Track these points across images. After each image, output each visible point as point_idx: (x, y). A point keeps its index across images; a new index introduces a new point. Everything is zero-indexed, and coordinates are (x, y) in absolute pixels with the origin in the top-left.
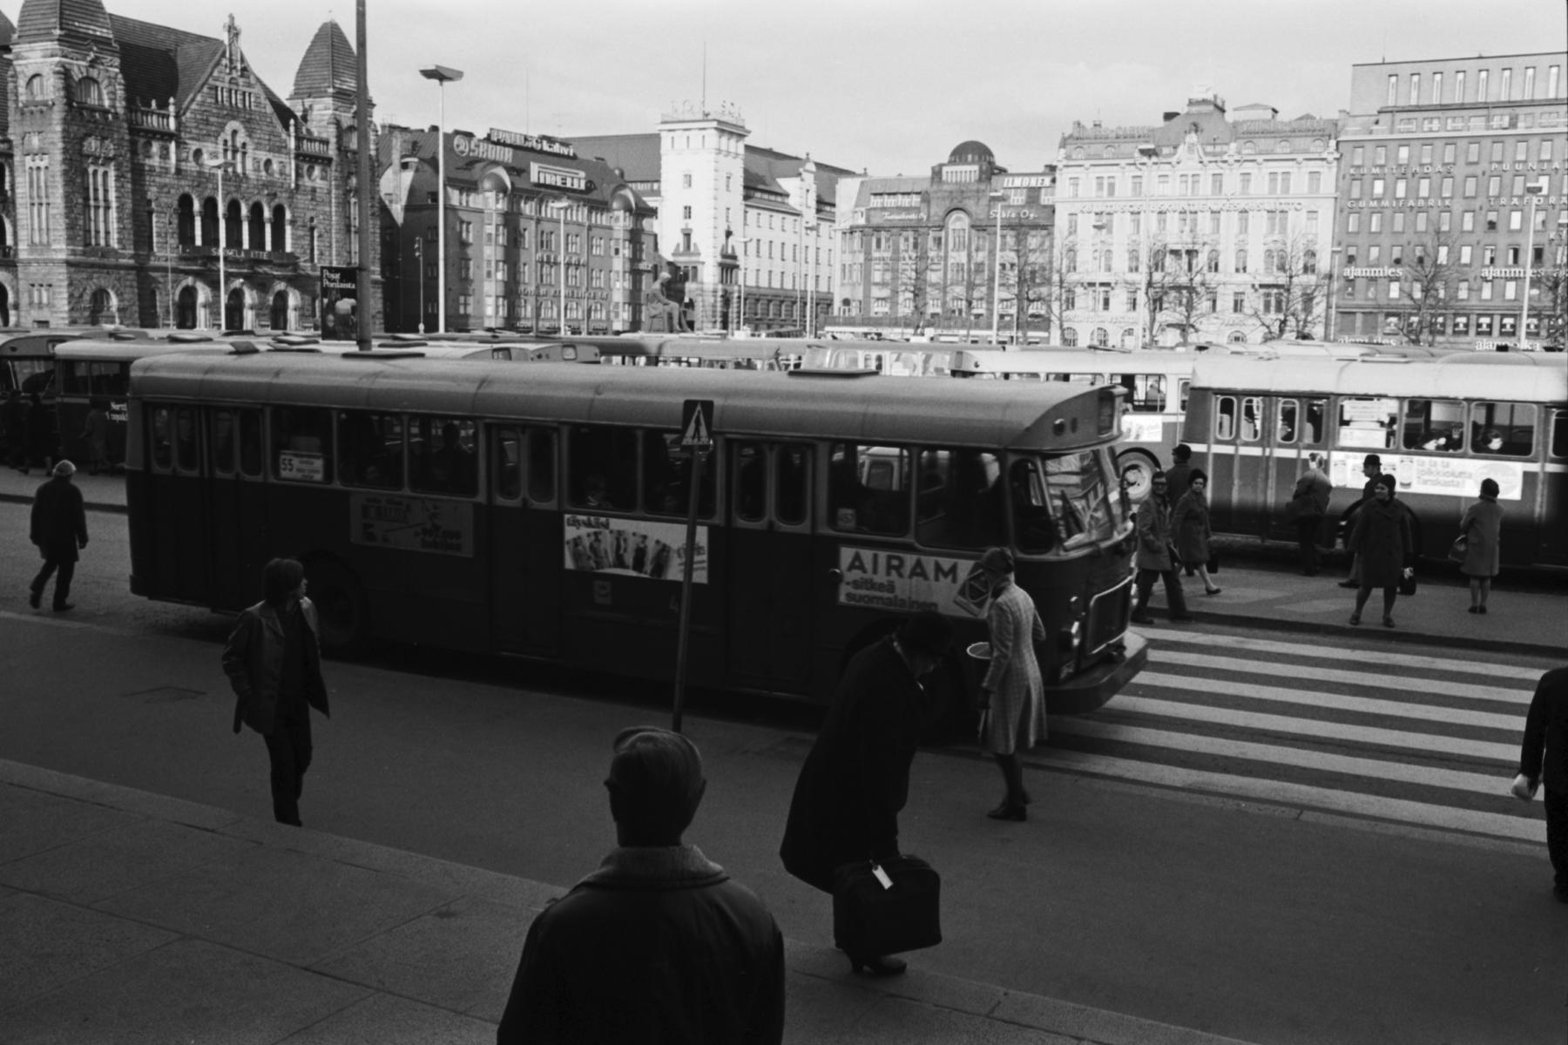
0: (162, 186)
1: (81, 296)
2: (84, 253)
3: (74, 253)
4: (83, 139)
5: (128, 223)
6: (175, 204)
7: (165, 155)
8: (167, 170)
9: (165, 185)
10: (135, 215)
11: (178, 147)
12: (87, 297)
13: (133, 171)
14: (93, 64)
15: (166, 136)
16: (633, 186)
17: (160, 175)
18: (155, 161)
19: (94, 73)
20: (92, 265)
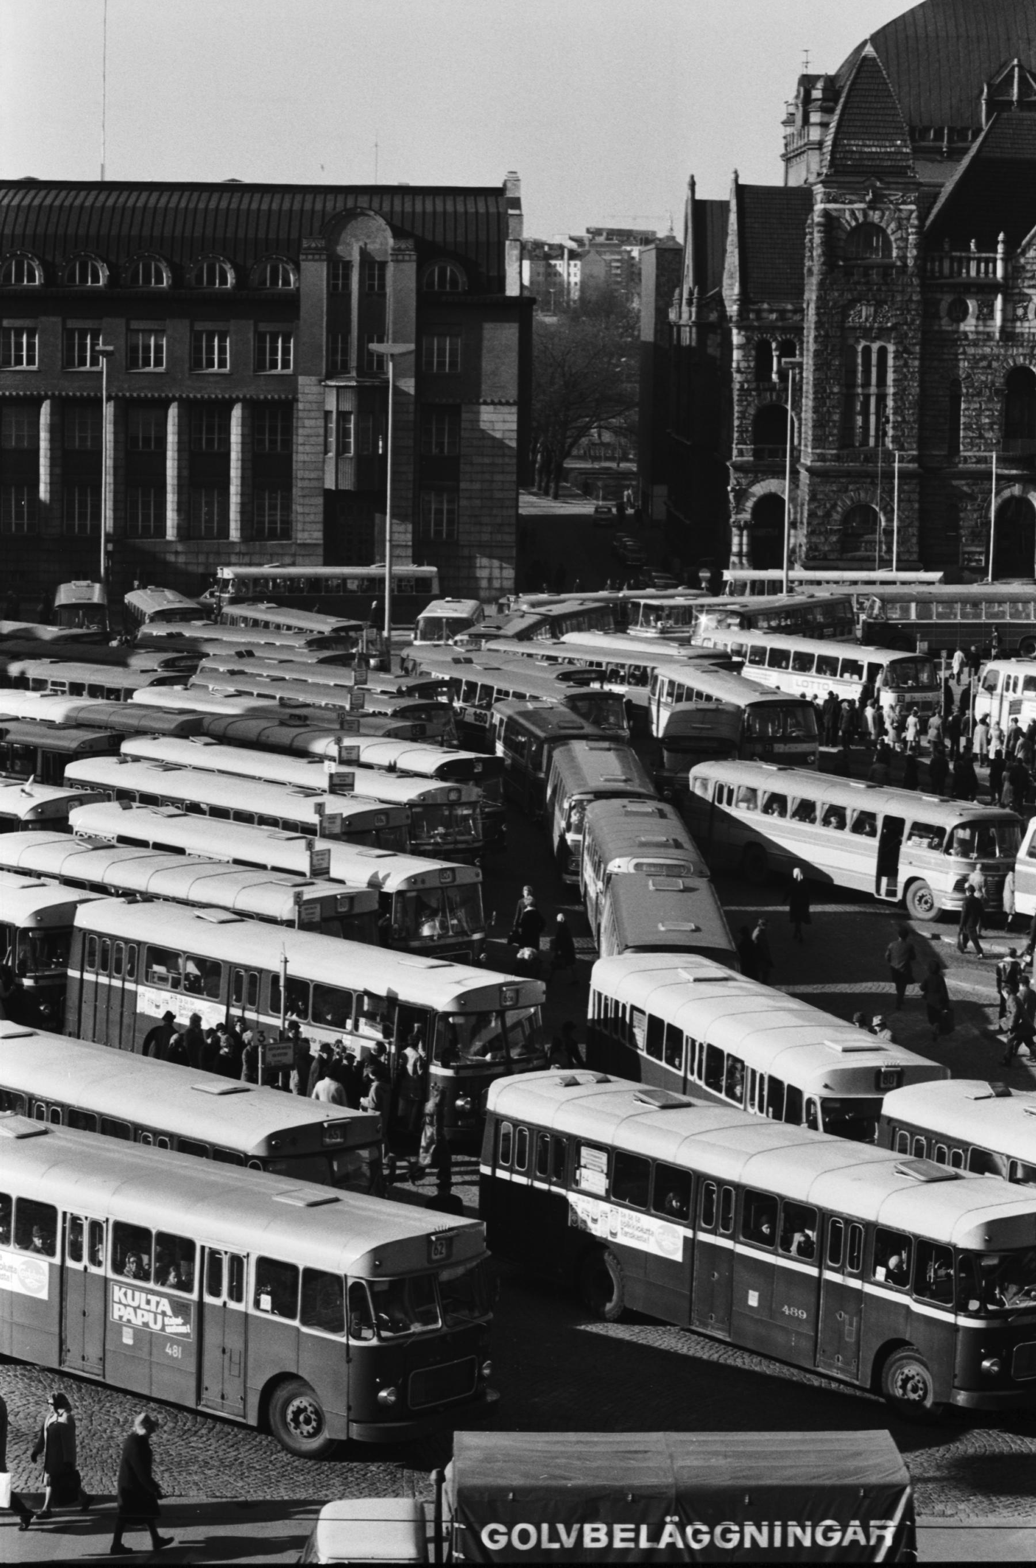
0: (975, 361)
1: (828, 514)
2: (838, 458)
3: (821, 458)
4: (852, 303)
5: (910, 414)
6: (999, 382)
7: (986, 315)
8: (989, 336)
9: (984, 357)
10: (923, 403)
11: (1005, 302)
12: (836, 517)
13: (923, 343)
14: (872, 206)
15: (986, 290)
16: (574, 425)
17: (975, 344)
18: (969, 325)
19: (875, 216)
20: (848, 474)
